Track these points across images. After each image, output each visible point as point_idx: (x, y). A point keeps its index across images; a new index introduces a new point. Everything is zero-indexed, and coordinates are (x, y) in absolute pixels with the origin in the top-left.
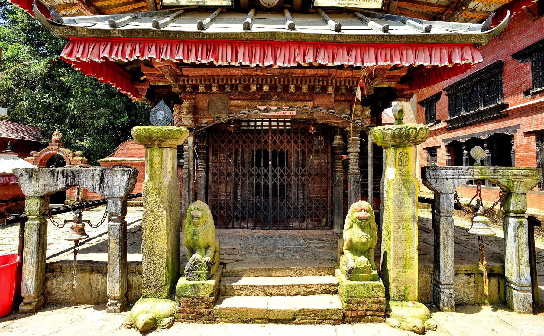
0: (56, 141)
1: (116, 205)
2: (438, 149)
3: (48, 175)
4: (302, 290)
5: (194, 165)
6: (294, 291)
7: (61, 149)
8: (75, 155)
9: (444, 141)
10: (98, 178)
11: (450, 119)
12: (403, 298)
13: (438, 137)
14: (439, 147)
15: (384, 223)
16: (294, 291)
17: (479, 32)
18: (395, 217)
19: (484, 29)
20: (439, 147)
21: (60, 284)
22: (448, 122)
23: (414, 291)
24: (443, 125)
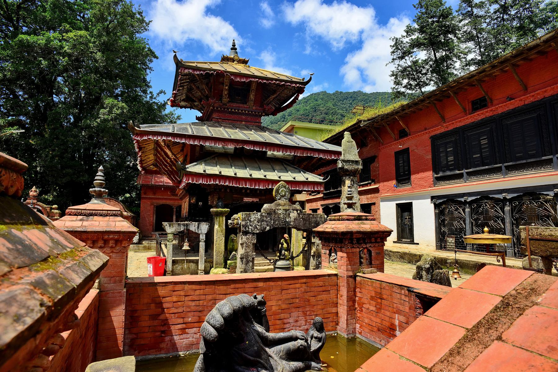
0: (33, 196)
1: (203, 236)
2: (318, 210)
3: (177, 225)
4: (267, 264)
5: (75, 215)
6: (264, 265)
7: (39, 203)
8: (51, 209)
9: (322, 205)
10: (197, 226)
11: (325, 192)
12: (298, 265)
13: (318, 202)
14: (319, 209)
15: (292, 242)
16: (264, 265)
17: (322, 181)
18: (296, 239)
19: (323, 180)
20: (319, 209)
21: (177, 267)
22: (323, 193)
23: (301, 263)
24: (321, 195)
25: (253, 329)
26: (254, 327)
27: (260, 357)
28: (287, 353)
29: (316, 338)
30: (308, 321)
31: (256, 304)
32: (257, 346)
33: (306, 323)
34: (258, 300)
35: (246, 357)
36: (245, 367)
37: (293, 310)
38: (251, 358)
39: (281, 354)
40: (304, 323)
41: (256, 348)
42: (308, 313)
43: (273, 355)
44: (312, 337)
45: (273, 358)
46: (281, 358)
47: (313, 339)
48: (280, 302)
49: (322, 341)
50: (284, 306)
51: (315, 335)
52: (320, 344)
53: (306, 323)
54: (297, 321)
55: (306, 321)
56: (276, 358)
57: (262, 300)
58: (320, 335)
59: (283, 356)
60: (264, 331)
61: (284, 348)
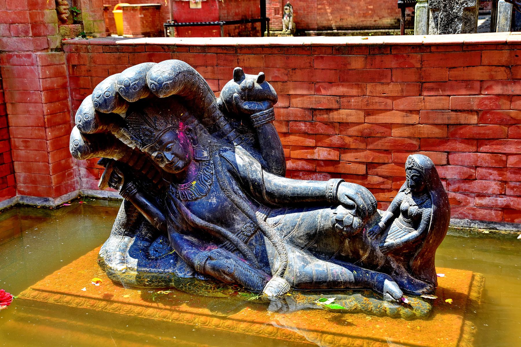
25: (221, 156)
26: (225, 150)
27: (228, 223)
28: (307, 234)
29: (405, 213)
30: (512, 184)
31: (235, 95)
32: (218, 197)
33: (503, 189)
34: (243, 83)
35: (187, 214)
36: (194, 240)
37: (459, 146)
38: (199, 221)
39: (294, 233)
40: (494, 187)
41: (214, 201)
42: (512, 160)
43: (272, 231)
44: (397, 212)
45: (270, 238)
46: (292, 242)
47: (401, 216)
48: (414, 119)
49: (422, 226)
50: (427, 130)
51: (403, 206)
52: (415, 233)
53: (503, 189)
54: (469, 179)
55: (504, 182)
56: (277, 238)
57: (258, 86)
58: (414, 209)
59: (299, 238)
60: (257, 166)
61: (303, 220)
